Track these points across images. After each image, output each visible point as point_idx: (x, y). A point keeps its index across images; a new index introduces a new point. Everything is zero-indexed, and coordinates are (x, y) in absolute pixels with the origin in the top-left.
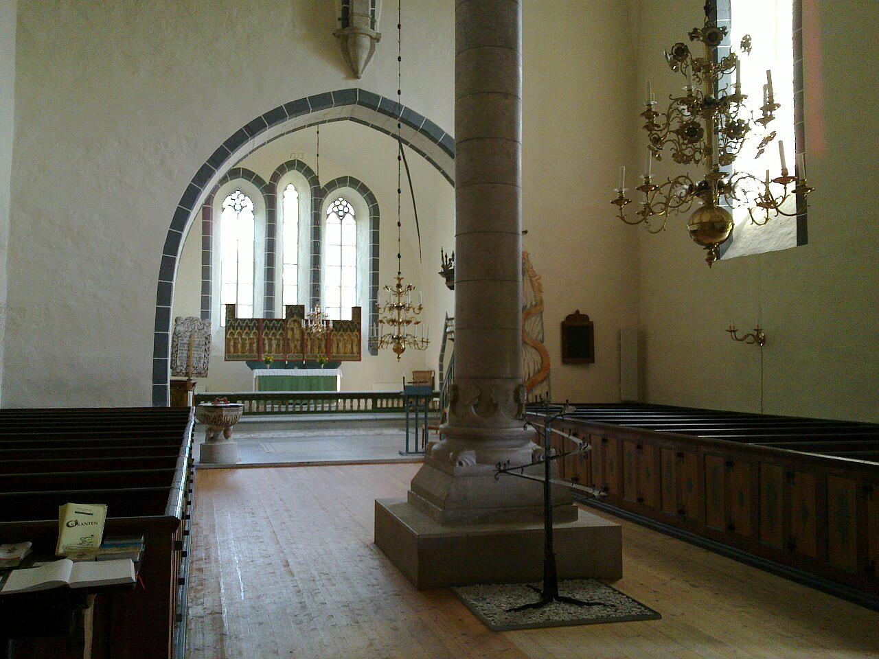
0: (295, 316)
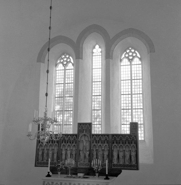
0: (85, 131)
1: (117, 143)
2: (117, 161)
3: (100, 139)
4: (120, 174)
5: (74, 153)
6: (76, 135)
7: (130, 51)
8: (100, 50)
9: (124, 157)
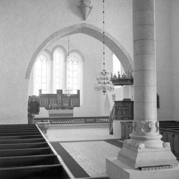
5: (55, 101)
6: (56, 94)
9: (75, 102)
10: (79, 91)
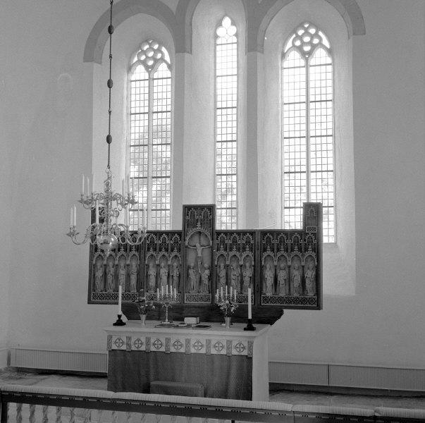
1: (272, 250)
2: (274, 290)
3: (235, 241)
4: (279, 317)
5: (175, 273)
6: (179, 233)
7: (307, 33)
8: (233, 30)
9: (289, 280)
10: (313, 212)
